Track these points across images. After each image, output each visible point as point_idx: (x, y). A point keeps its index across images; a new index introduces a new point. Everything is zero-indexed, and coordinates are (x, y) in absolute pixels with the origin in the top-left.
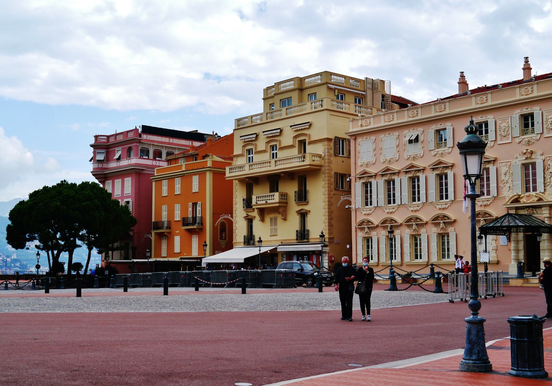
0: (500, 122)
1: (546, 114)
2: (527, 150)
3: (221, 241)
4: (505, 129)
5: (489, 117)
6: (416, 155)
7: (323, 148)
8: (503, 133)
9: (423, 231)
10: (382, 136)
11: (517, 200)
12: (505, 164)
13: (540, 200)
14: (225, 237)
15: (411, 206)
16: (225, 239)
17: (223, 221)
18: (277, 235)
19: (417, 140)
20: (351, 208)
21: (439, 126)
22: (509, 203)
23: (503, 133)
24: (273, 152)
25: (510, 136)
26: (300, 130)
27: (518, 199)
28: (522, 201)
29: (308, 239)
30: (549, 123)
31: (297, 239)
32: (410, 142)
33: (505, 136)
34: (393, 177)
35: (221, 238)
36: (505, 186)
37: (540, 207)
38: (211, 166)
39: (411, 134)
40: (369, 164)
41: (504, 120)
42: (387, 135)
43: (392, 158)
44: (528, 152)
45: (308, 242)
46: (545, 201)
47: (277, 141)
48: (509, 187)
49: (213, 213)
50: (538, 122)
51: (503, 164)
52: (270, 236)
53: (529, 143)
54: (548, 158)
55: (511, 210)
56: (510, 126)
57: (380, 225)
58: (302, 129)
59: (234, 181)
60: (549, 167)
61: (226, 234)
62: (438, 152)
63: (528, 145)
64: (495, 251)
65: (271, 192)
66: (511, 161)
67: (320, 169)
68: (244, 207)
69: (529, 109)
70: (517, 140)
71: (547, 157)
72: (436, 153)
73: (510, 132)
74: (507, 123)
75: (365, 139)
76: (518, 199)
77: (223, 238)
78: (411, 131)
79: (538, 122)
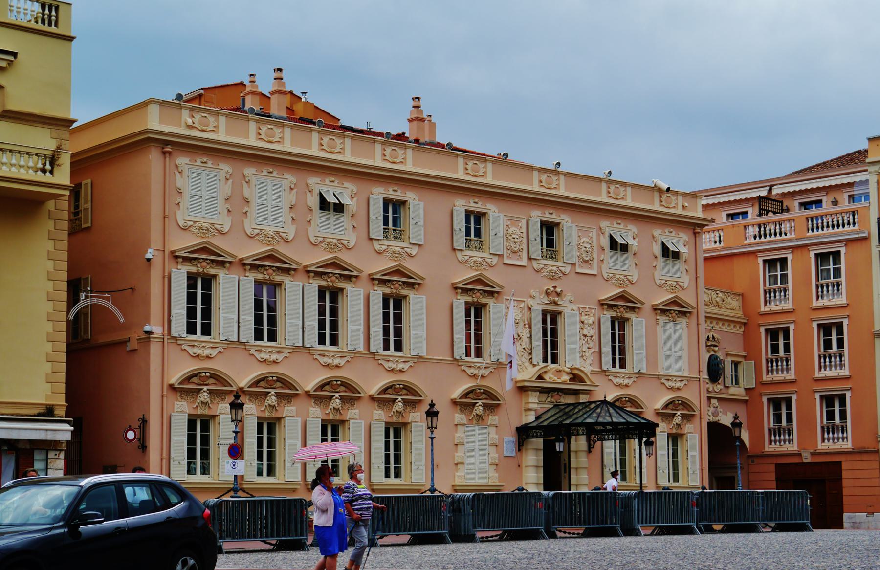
0: (509, 223)
1: (578, 234)
2: (555, 287)
4: (517, 239)
5: (489, 206)
8: (513, 245)
9: (352, 413)
10: (250, 171)
11: (540, 378)
15: (196, 344)
21: (391, 192)
22: (534, 379)
23: (513, 245)
25: (524, 254)
28: (546, 377)
30: (584, 251)
33: (515, 252)
34: (278, 278)
40: (213, 231)
41: (515, 222)
42: (265, 173)
43: (278, 233)
44: (556, 292)
46: (588, 383)
48: (524, 348)
50: (569, 244)
53: (553, 277)
54: (581, 310)
55: (533, 392)
56: (525, 235)
62: (389, 246)
63: (552, 279)
64: (494, 467)
66: (524, 301)
69: (554, 216)
70: (535, 265)
71: (578, 307)
72: (385, 247)
73: (525, 247)
74: (519, 227)
75: (198, 163)
78: (327, 182)
79: (569, 244)
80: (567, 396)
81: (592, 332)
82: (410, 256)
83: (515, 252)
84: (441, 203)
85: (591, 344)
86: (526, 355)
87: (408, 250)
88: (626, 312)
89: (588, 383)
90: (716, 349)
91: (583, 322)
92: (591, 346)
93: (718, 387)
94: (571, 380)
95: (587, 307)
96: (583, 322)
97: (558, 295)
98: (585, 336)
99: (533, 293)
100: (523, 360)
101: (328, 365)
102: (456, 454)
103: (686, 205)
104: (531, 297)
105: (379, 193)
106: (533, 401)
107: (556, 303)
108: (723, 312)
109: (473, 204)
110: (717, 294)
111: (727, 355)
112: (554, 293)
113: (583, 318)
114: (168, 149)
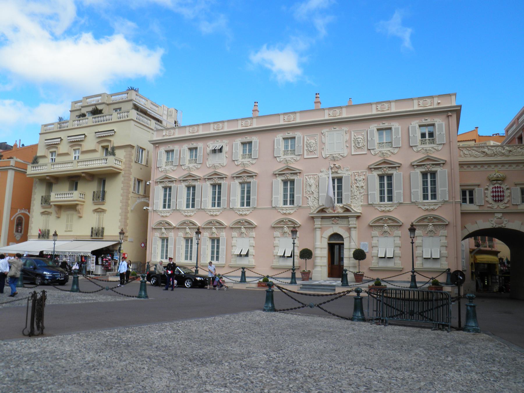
3: (16, 234)
6: (220, 164)
7: (124, 154)
8: (309, 148)
11: (322, 211)
12: (311, 176)
13: (347, 210)
14: (21, 230)
16: (21, 232)
17: (20, 215)
18: (72, 231)
19: (220, 150)
20: (148, 209)
22: (315, 212)
23: (309, 148)
24: (75, 155)
26: (104, 136)
27: (324, 210)
29: (102, 236)
31: (92, 236)
32: (214, 151)
33: (311, 152)
35: (17, 231)
36: (310, 197)
37: (347, 217)
38: (14, 165)
39: (217, 144)
45: (102, 239)
47: (81, 145)
49: (11, 208)
51: (310, 176)
52: (65, 231)
57: (177, 227)
58: (106, 136)
59: (34, 179)
60: (356, 181)
61: (21, 228)
65: (70, 190)
67: (120, 173)
68: (41, 204)
76: (324, 210)
77: (19, 231)
80: (343, 219)
81: (363, 184)
82: (252, 164)
83: (311, 152)
84: (267, 138)
85: (362, 191)
86: (316, 201)
87: (251, 162)
88: (389, 170)
89: (353, 212)
90: (500, 182)
91: (356, 180)
92: (362, 192)
93: (501, 205)
94: (345, 211)
95: (360, 171)
96: (356, 180)
97: (337, 168)
98: (358, 187)
99: (322, 170)
100: (315, 203)
101: (212, 215)
102: (274, 251)
103: (439, 101)
104: (321, 172)
105: (238, 141)
106: (318, 224)
107: (337, 173)
108: (511, 158)
109: (287, 134)
110: (504, 148)
111: (516, 185)
112: (335, 168)
113: (357, 177)
114: (157, 145)
